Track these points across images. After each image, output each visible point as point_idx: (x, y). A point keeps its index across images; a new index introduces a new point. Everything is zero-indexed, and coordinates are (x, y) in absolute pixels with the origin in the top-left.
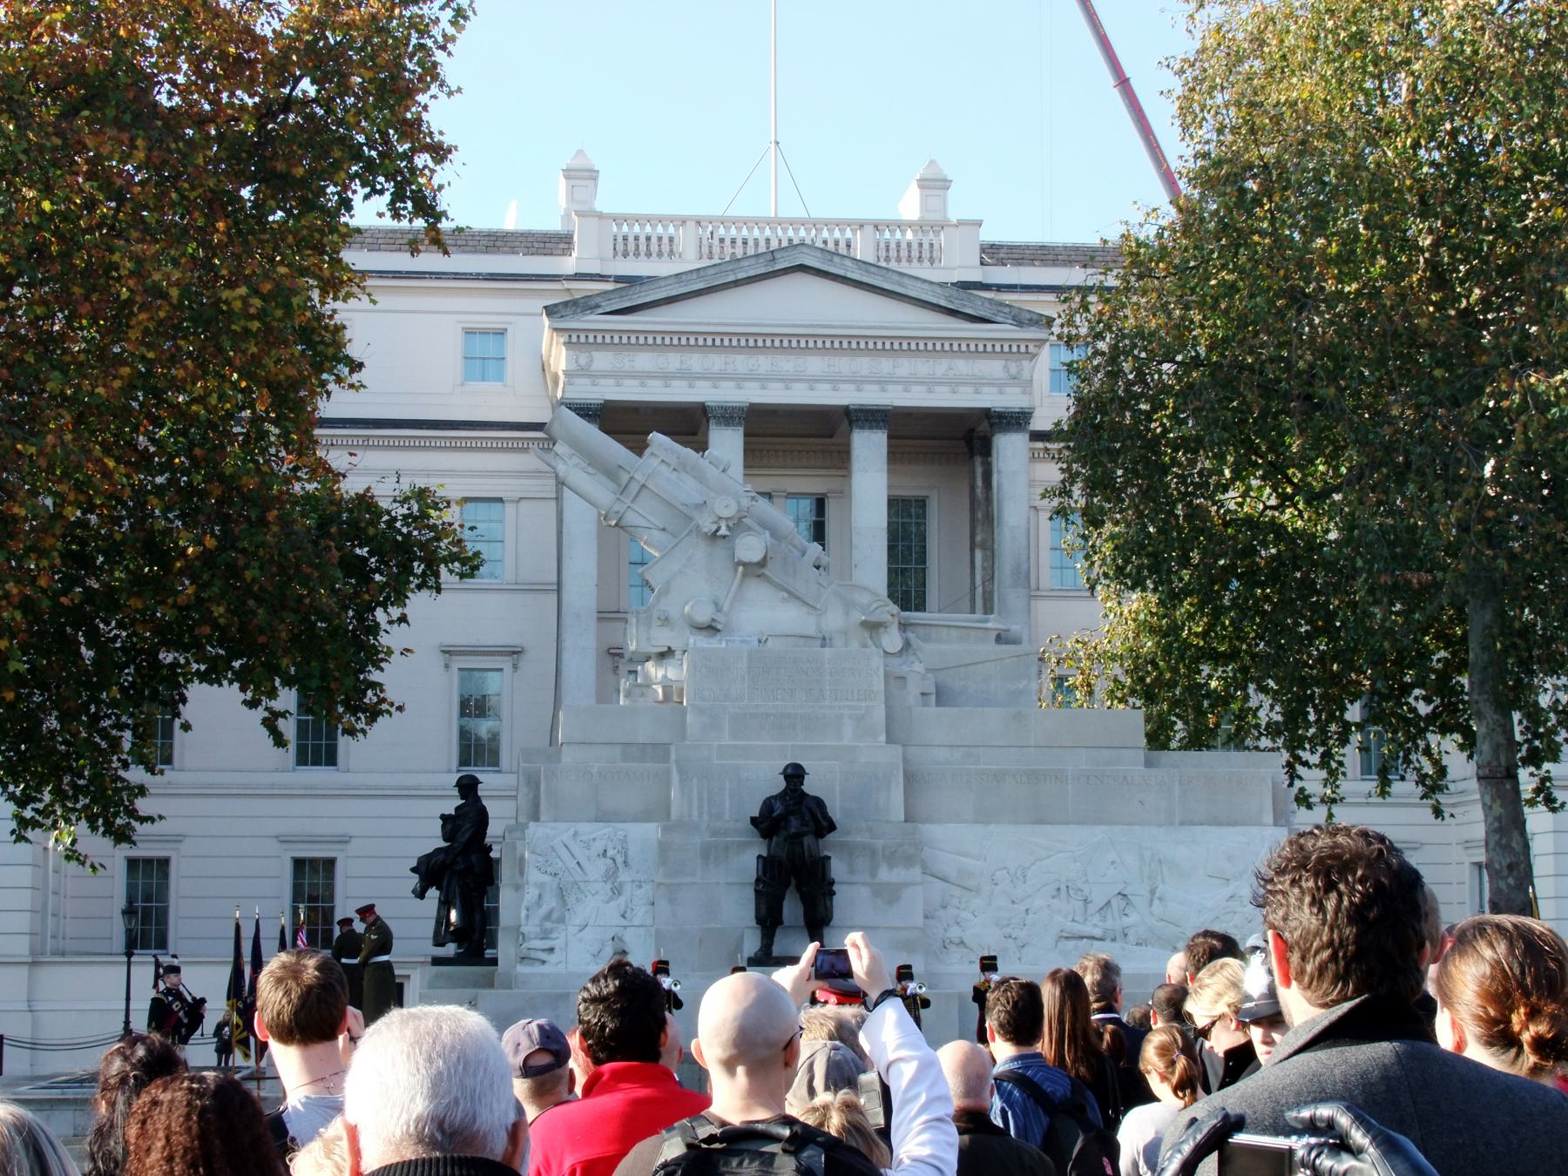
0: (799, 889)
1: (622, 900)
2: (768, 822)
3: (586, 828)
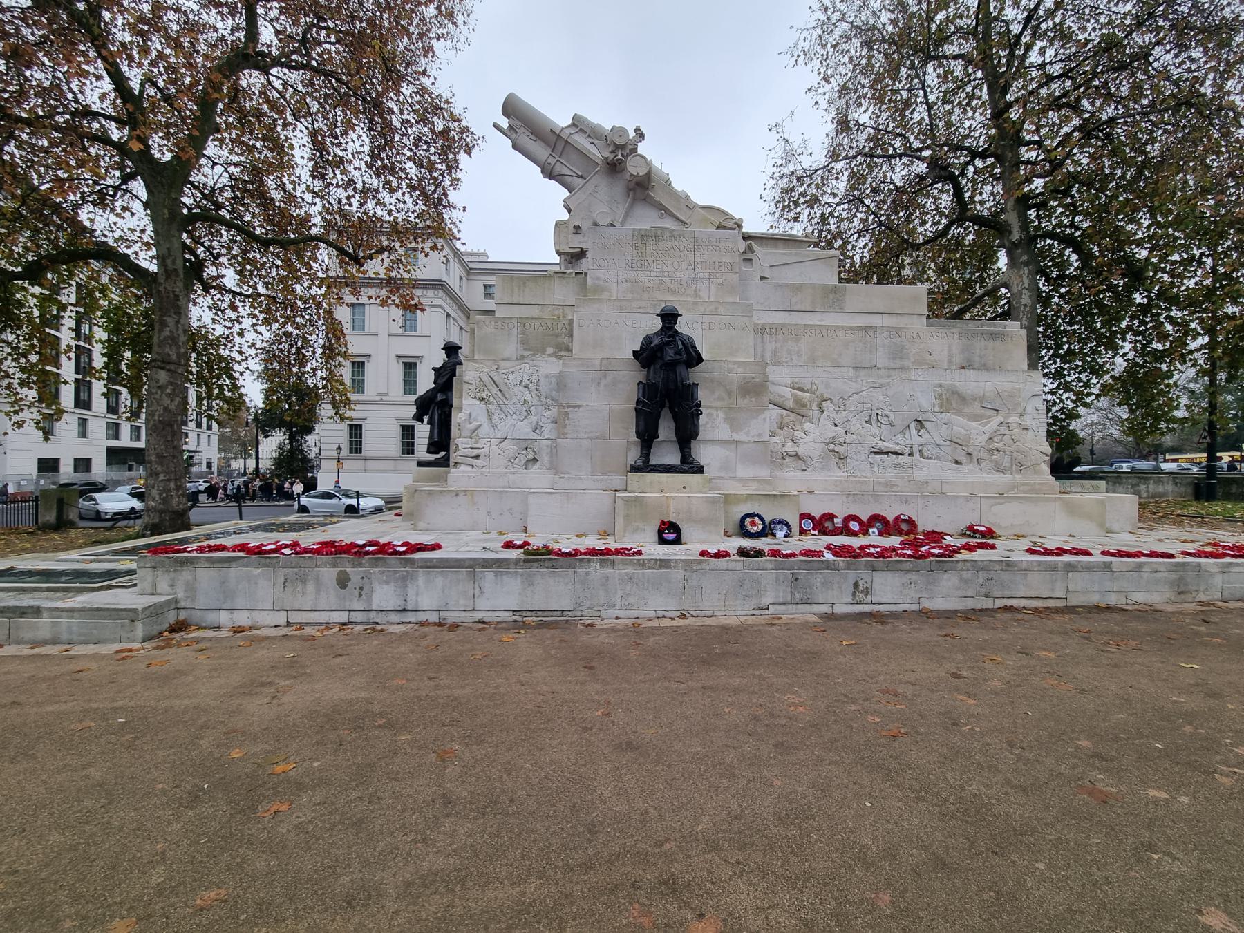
1: (534, 418)
2: (648, 355)
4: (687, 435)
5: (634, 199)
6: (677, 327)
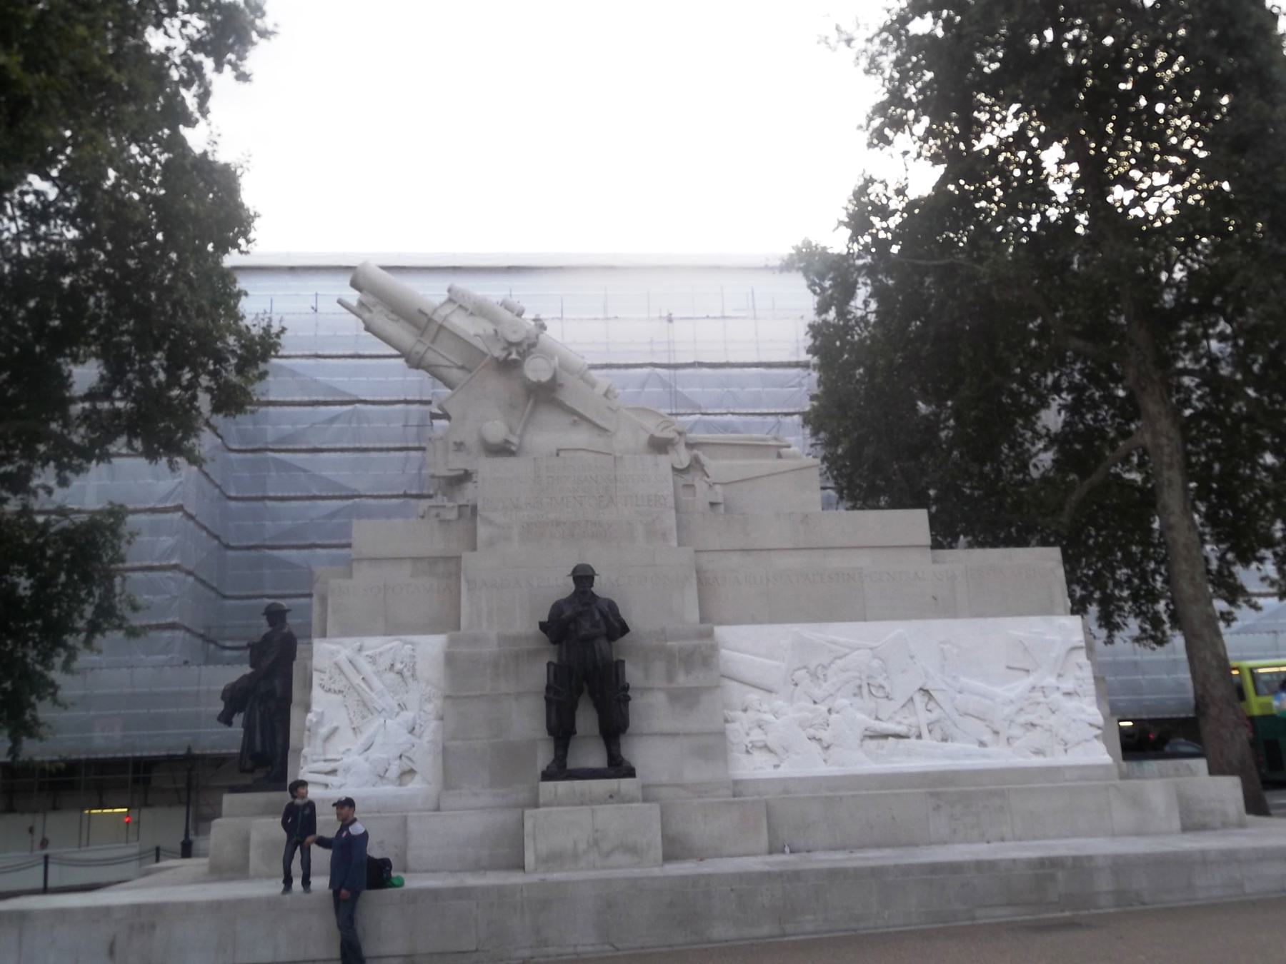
0: (592, 694)
3: (375, 644)
4: (614, 729)
5: (536, 403)
6: (593, 589)
